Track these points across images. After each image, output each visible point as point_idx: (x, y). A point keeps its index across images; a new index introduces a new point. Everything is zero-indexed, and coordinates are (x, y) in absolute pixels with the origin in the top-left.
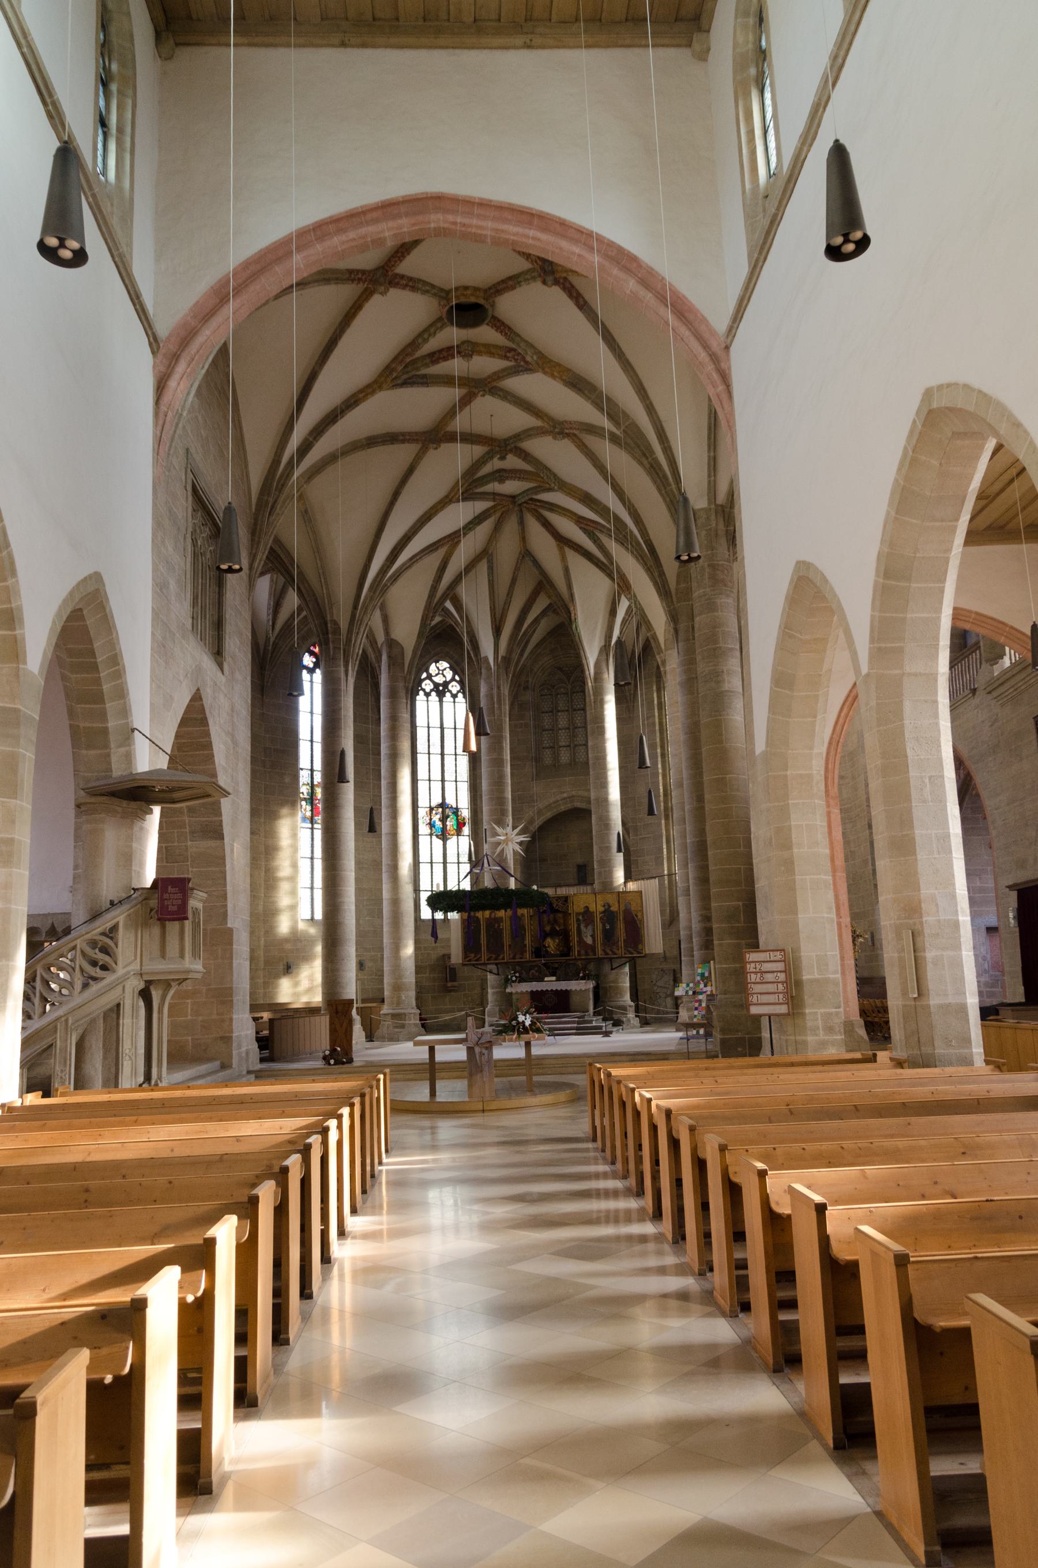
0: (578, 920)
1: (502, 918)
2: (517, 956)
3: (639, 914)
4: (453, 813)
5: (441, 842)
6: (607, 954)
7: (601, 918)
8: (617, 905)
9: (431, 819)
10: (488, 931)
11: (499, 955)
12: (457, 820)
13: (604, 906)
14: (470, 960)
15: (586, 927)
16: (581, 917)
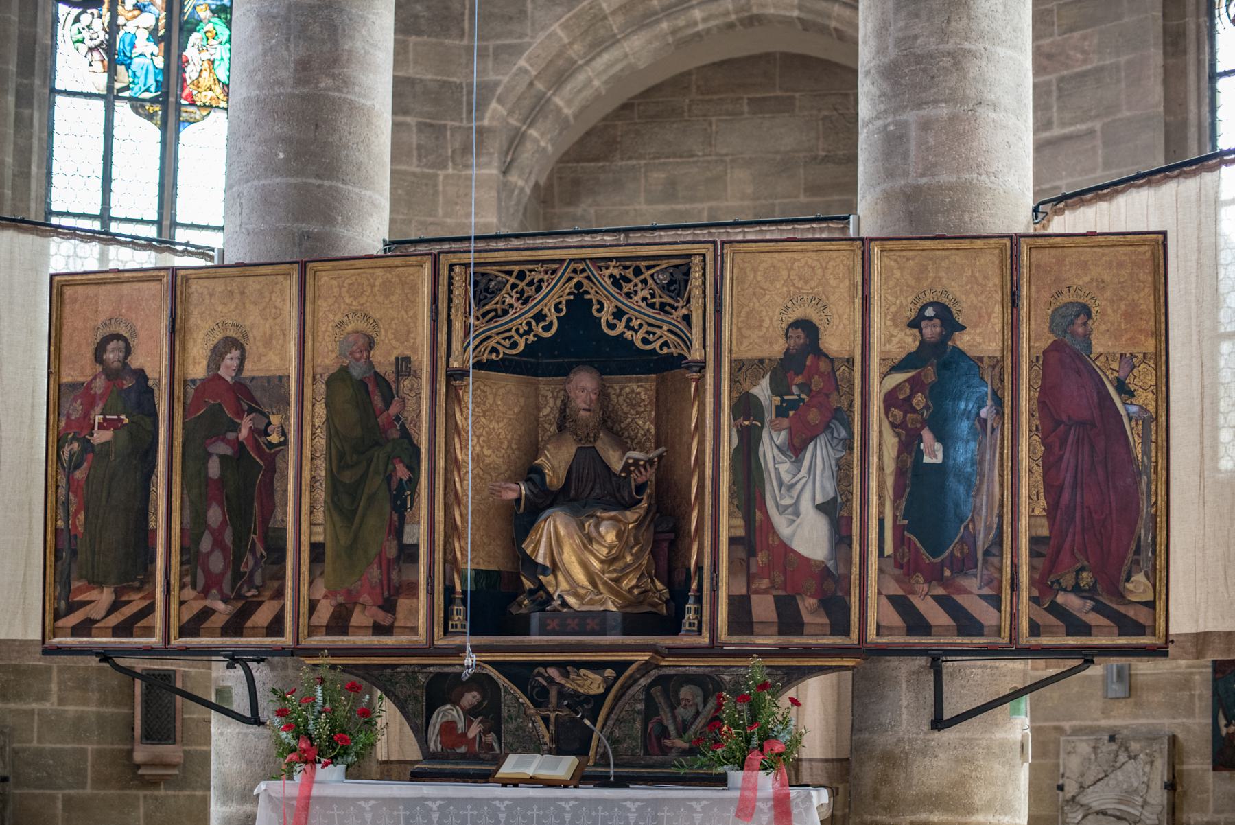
0: (746, 406)
1: (283, 380)
2: (357, 619)
3: (1143, 378)
5: (151, 133)
6: (917, 625)
7: (890, 400)
8: (997, 318)
10: (194, 456)
11: (249, 608)
13: (915, 324)
14: (84, 628)
15: (795, 449)
16: (762, 390)
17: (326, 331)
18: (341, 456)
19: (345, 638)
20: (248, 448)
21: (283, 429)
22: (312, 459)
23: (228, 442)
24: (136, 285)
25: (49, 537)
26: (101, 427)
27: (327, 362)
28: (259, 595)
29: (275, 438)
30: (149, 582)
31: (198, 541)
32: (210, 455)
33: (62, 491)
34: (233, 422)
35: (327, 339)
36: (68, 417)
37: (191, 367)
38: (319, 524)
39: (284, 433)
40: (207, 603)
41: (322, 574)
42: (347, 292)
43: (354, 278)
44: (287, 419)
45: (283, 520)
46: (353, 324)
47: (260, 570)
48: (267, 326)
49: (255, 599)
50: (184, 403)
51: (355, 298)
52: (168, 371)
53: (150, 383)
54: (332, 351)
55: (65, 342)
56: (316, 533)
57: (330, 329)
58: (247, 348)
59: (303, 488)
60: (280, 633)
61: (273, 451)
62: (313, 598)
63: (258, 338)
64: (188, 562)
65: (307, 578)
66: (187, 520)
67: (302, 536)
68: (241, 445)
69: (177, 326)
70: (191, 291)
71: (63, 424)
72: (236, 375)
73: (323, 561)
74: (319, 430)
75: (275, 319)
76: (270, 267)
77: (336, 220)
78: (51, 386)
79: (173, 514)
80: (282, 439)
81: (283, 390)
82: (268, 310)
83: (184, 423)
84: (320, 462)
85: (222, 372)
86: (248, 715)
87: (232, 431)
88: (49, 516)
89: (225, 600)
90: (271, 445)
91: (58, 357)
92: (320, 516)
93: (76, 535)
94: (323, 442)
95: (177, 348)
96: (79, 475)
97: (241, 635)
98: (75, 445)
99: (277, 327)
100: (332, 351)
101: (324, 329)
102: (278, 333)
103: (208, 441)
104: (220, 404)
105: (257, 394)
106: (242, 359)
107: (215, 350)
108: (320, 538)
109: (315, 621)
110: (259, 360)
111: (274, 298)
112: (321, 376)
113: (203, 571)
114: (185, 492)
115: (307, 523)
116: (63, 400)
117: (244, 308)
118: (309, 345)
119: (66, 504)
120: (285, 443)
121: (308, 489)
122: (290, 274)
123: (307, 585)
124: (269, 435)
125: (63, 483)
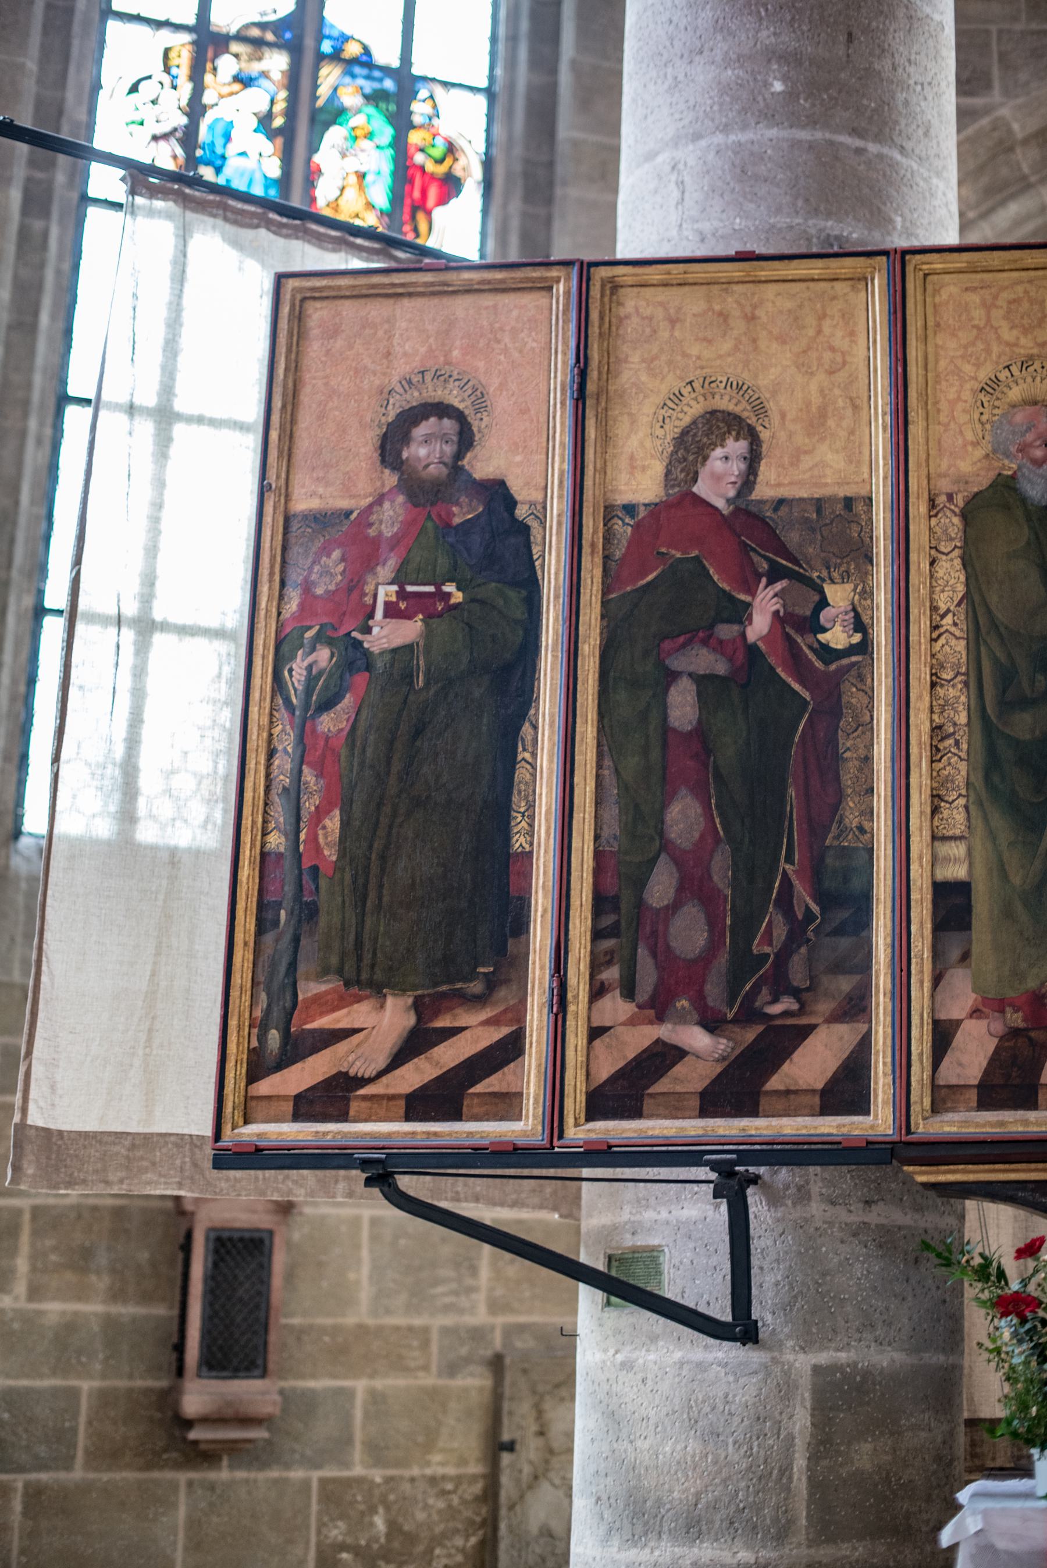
4: (374, 98)
9: (195, 109)
12: (400, 147)
17: (959, 398)
18: (1006, 677)
19: (1032, 1115)
20: (772, 660)
21: (857, 617)
22: (933, 685)
23: (720, 647)
24: (488, 300)
25: (245, 872)
26: (392, 611)
27: (965, 467)
28: (802, 1011)
29: (837, 637)
30: (507, 981)
31: (640, 882)
32: (673, 676)
33: (283, 763)
34: (731, 599)
35: (963, 418)
36: (307, 588)
37: (624, 477)
38: (954, 838)
39: (860, 625)
40: (664, 1031)
41: (965, 957)
42: (1006, 318)
43: (1020, 289)
44: (867, 594)
45: (861, 829)
46: (1023, 386)
47: (803, 950)
48: (813, 387)
49: (790, 1021)
50: (606, 558)
51: (1026, 331)
52: (568, 483)
53: (521, 512)
54: (976, 444)
55: (306, 419)
56: (947, 860)
57: (967, 395)
58: (764, 435)
59: (914, 750)
60: (860, 1104)
61: (833, 667)
62: (942, 1016)
63: (789, 417)
64: (614, 931)
65: (928, 967)
66: (612, 828)
67: (914, 867)
68: (752, 650)
69: (591, 387)
70: (622, 312)
71: (292, 606)
72: (739, 494)
73: (968, 927)
74: (948, 620)
75: (831, 373)
76: (819, 263)
77: (891, 221)
78: (268, 519)
79: (577, 816)
80: (857, 638)
81: (855, 528)
82: (813, 355)
83: (604, 604)
84: (952, 692)
85: (701, 489)
86: (722, 1311)
87: (729, 621)
88: (247, 822)
89: (712, 1024)
90: (827, 653)
91: (288, 454)
92: (955, 817)
93: (315, 870)
94: (961, 646)
95: (591, 432)
96: (329, 723)
97: (754, 1113)
98: (323, 656)
99: (837, 392)
100: (976, 444)
101: (952, 396)
102: (840, 403)
103: (667, 645)
104: (697, 558)
105: (792, 538)
106: (753, 459)
107: (683, 439)
108: (958, 872)
109: (949, 1073)
110: (795, 461)
111: (827, 330)
112: (950, 497)
113: (654, 954)
114: (607, 762)
115: (927, 834)
116: (295, 551)
117: (756, 349)
118: (916, 431)
119: (295, 794)
120: (865, 647)
121: (926, 754)
122: (864, 279)
123: (927, 985)
124: (824, 630)
125: (287, 742)
